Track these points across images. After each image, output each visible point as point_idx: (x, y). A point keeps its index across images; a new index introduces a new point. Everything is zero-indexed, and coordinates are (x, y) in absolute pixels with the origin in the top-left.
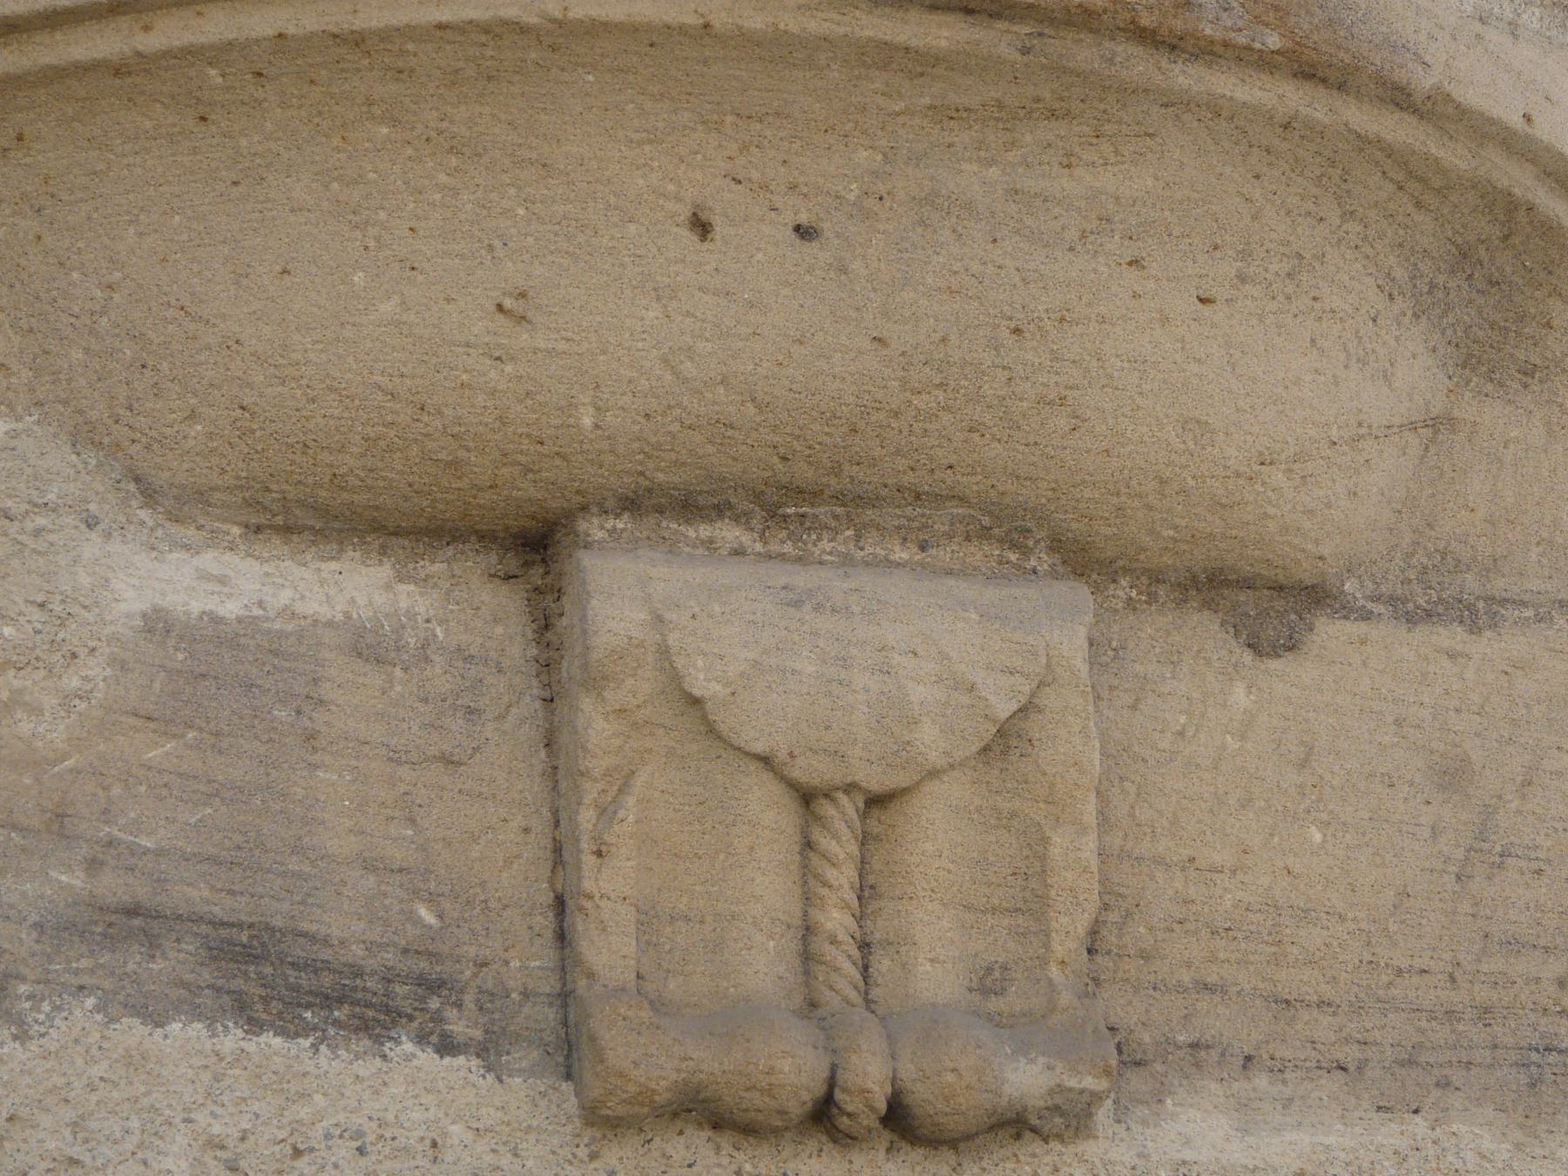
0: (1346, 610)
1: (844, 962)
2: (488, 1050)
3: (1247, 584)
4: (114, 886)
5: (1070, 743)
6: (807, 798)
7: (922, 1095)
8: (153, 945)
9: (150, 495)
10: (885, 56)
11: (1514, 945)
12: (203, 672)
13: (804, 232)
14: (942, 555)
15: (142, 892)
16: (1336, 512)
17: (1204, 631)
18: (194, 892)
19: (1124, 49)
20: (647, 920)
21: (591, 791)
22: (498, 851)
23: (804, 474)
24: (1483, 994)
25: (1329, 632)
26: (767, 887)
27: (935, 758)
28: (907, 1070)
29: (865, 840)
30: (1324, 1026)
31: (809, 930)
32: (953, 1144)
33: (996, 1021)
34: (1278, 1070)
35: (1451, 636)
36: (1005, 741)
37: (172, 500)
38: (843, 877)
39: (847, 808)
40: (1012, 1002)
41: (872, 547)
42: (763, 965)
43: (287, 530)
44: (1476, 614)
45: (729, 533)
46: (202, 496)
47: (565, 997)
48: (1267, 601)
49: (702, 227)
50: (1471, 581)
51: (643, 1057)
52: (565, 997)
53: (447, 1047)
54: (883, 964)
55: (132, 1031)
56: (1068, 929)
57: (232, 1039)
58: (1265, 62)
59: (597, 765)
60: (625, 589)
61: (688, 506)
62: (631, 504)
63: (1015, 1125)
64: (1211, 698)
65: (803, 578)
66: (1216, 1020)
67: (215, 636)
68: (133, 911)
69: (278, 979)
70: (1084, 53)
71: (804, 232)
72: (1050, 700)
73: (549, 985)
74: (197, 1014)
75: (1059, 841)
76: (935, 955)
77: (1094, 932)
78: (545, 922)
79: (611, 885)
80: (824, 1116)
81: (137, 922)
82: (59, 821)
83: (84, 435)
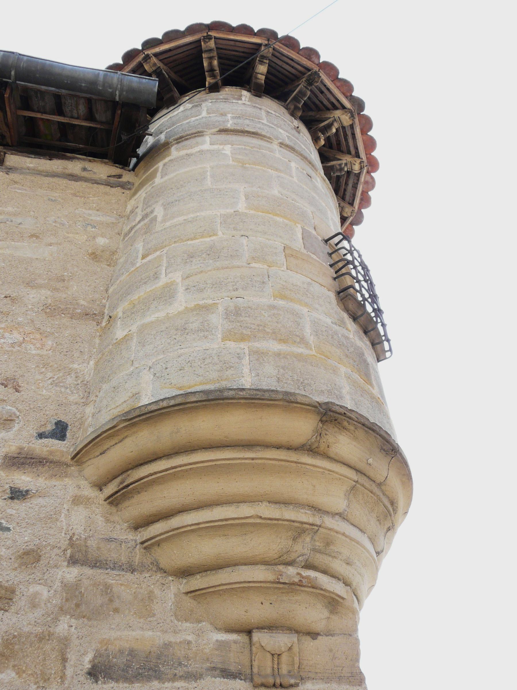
0: (321, 635)
1: (276, 670)
2: (245, 680)
3: (312, 633)
4: (212, 665)
5: (296, 649)
6: (273, 655)
7: (283, 683)
8: (215, 671)
9: (217, 629)
10: (276, 588)
11: (337, 667)
12: (221, 645)
13: (271, 604)
14: (284, 632)
15: (214, 665)
16: (319, 627)
17: (308, 638)
18: (219, 666)
19: (297, 586)
20: (259, 667)
21: (254, 655)
22: (245, 660)
23: (272, 625)
24: (334, 671)
25: (320, 637)
26: (269, 663)
27: (284, 651)
28: (282, 681)
29: (278, 659)
30: (320, 675)
31: (273, 667)
32: (287, 688)
33: (290, 676)
34: (316, 679)
35: (330, 637)
36: (290, 649)
37: (219, 629)
38: (276, 662)
39: (276, 656)
40: (292, 674)
41: (278, 631)
42: (269, 671)
43: (228, 632)
44: (332, 635)
45: (266, 631)
46: (221, 629)
47: (252, 675)
48: (314, 635)
49: (262, 603)
50: (332, 632)
51: (258, 680)
52: (252, 675)
53: (241, 680)
54: (280, 670)
55: (213, 679)
56: (296, 666)
57: (222, 679)
58: (309, 587)
59: (254, 652)
60: (256, 636)
61: (262, 628)
62: (257, 628)
63: (292, 686)
64: (309, 644)
65: (272, 634)
66: (310, 675)
67: (223, 642)
68: (214, 667)
69: (227, 674)
70: (293, 587)
71: (271, 604)
72: (294, 645)
73: (250, 673)
74: (219, 677)
75: (295, 658)
76: (284, 669)
77: (299, 666)
78: (250, 667)
79: (255, 664)
80: (274, 685)
81: (214, 669)
82: (208, 659)
83: (211, 624)
